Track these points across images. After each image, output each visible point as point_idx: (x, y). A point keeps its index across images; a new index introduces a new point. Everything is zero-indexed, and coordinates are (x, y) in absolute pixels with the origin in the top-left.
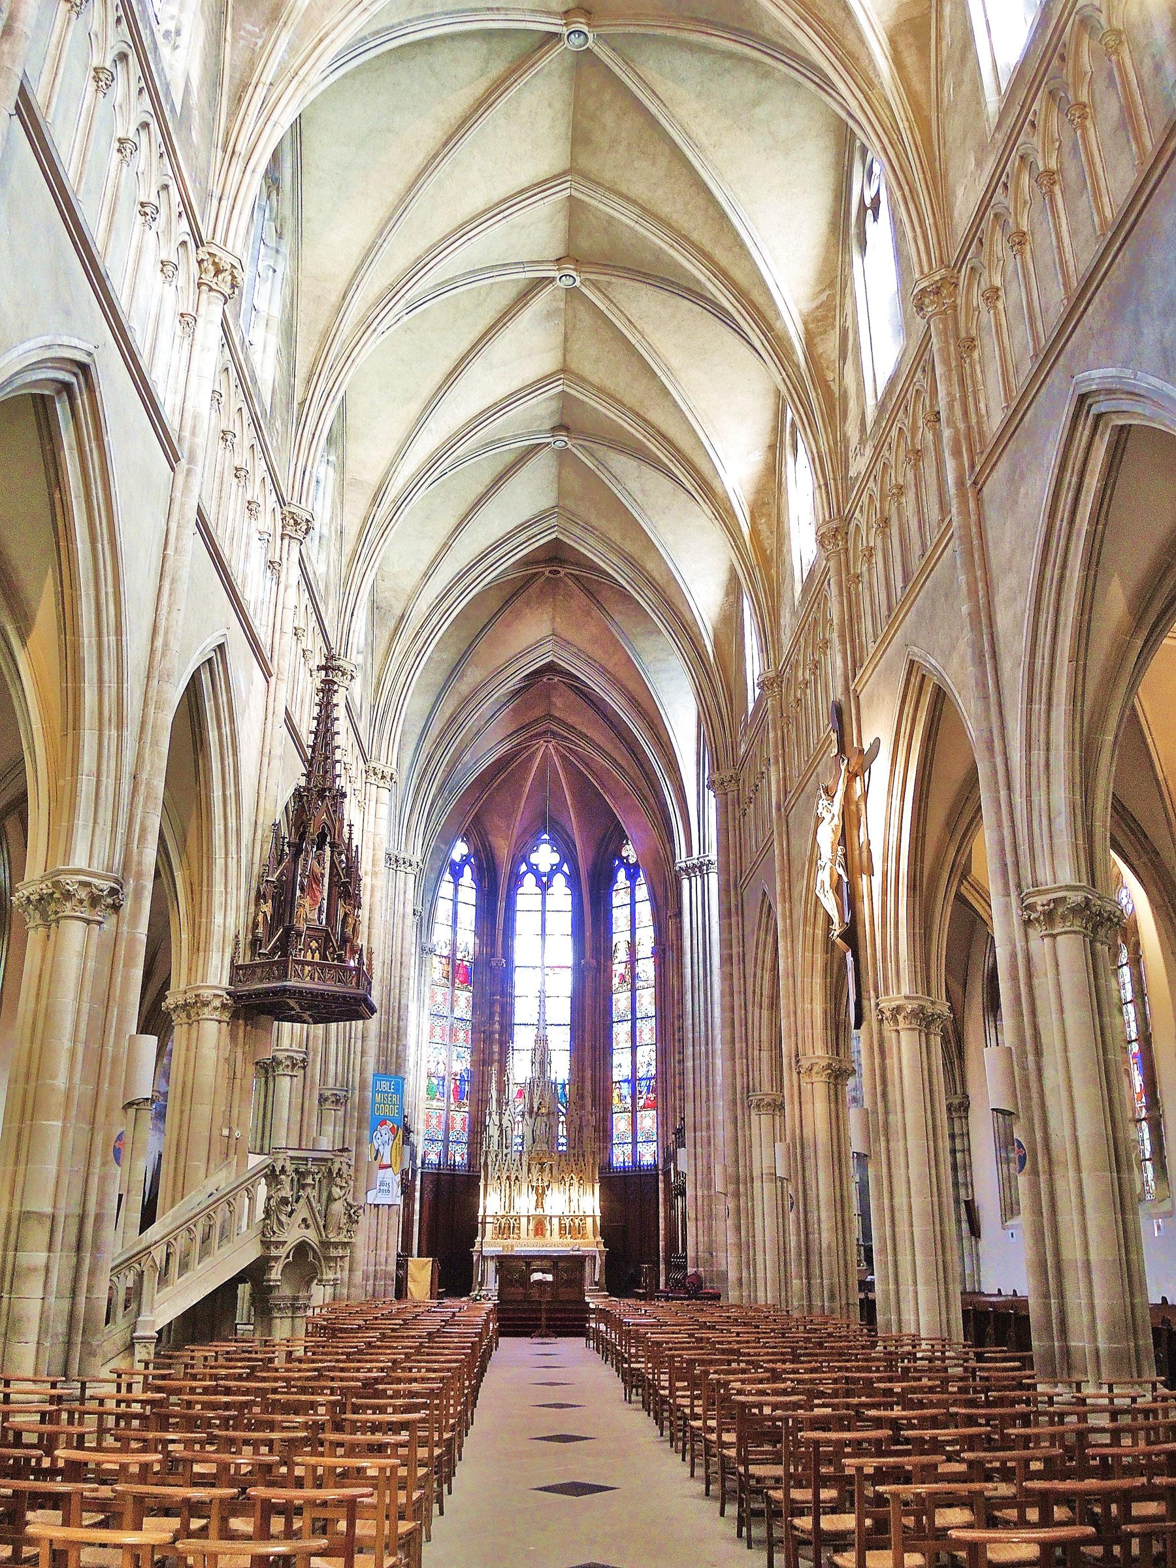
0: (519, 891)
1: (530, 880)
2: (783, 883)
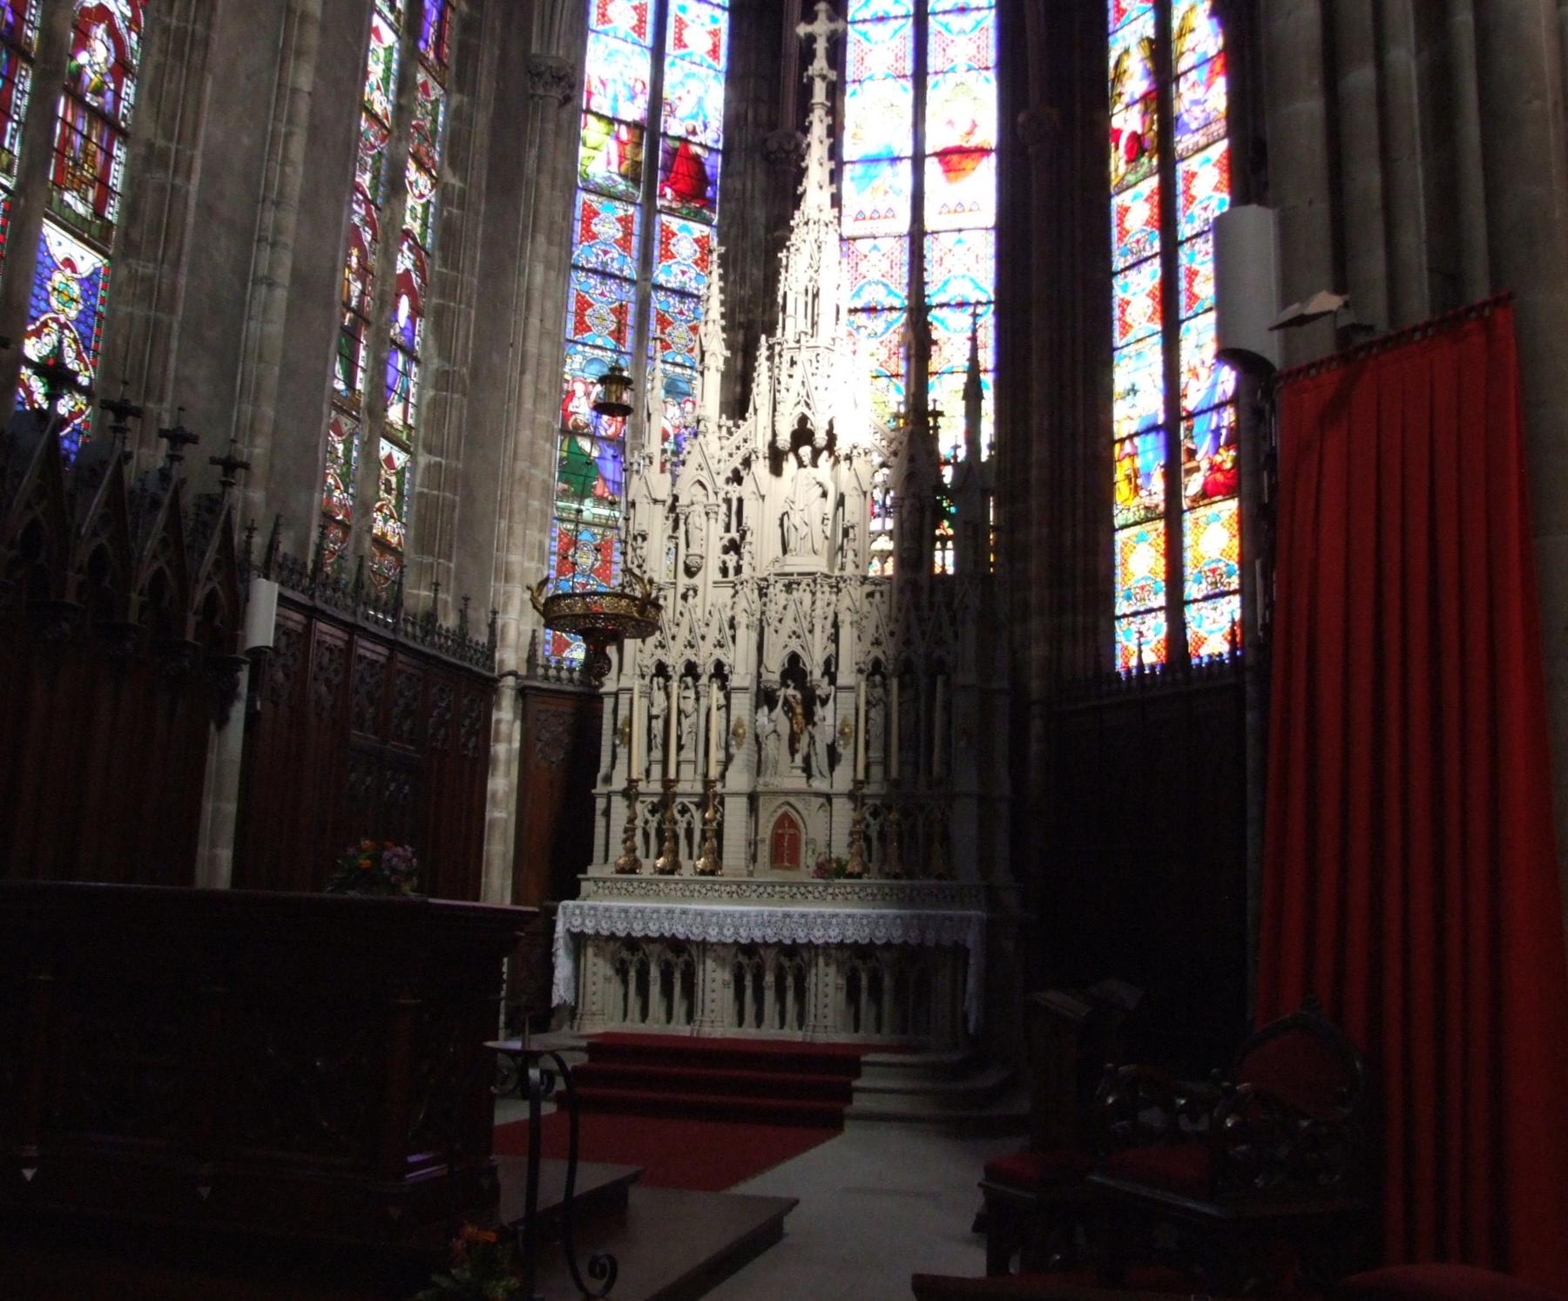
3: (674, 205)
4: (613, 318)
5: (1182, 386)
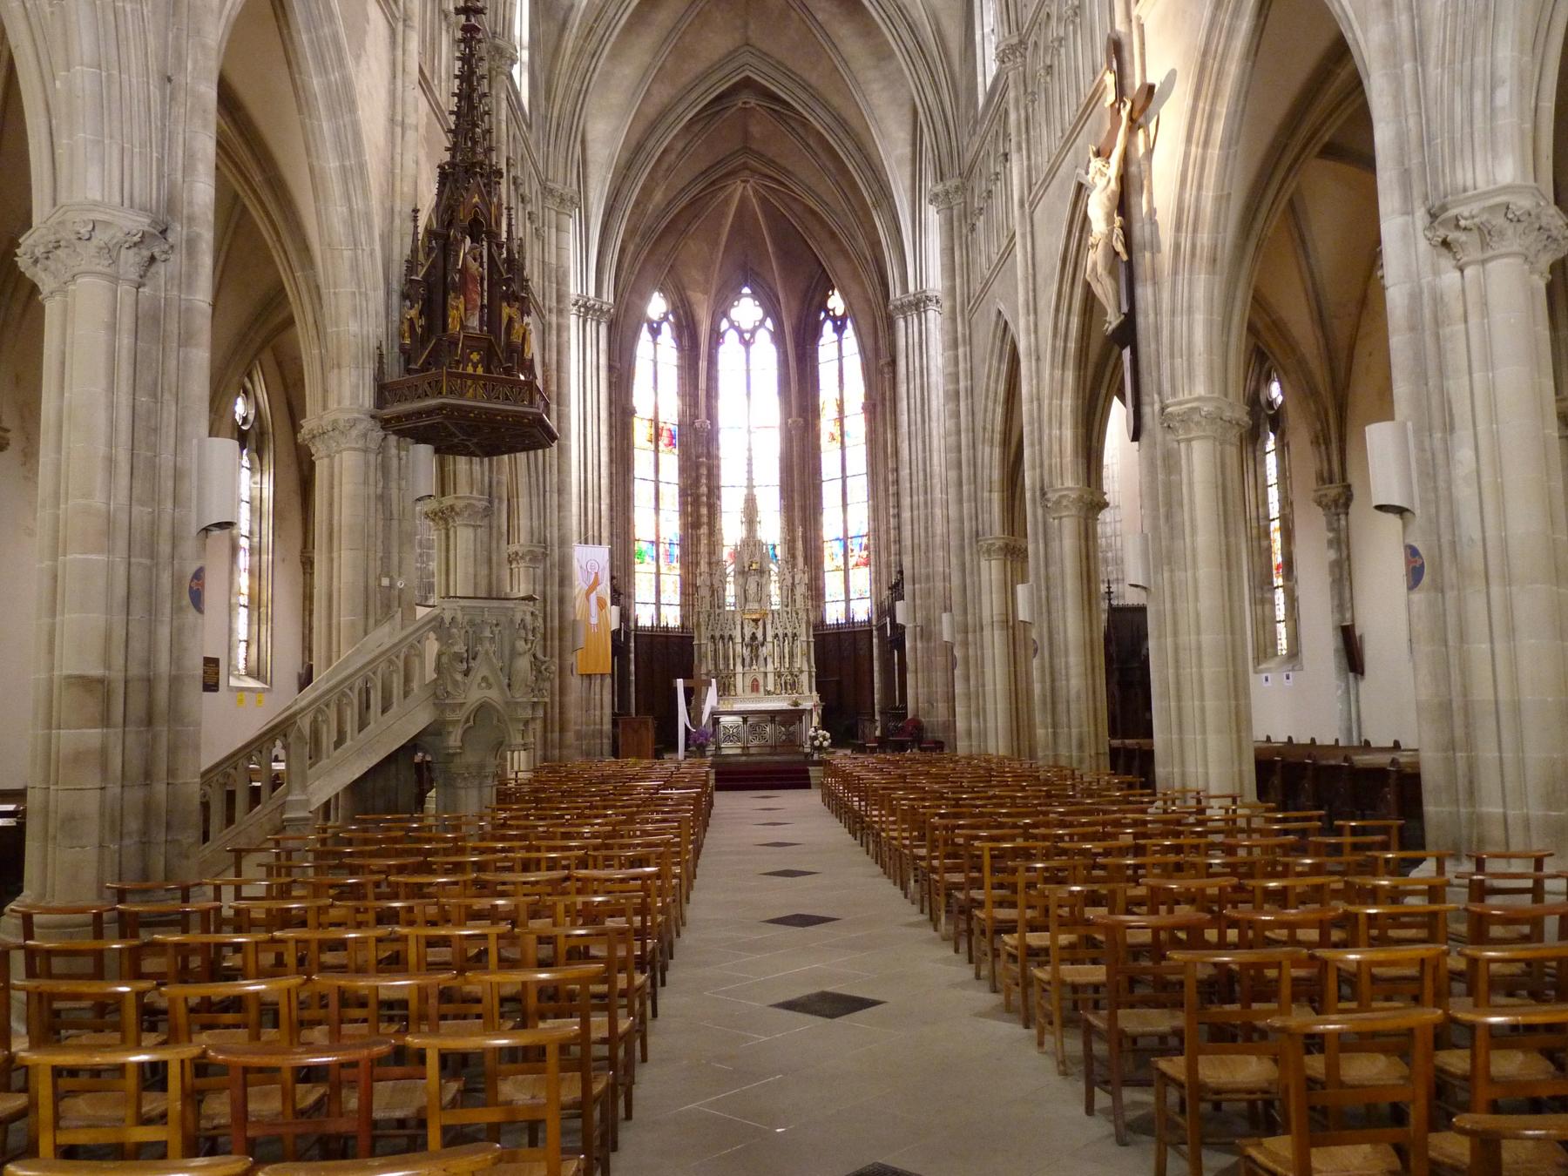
1: (731, 338)
2: (1027, 293)
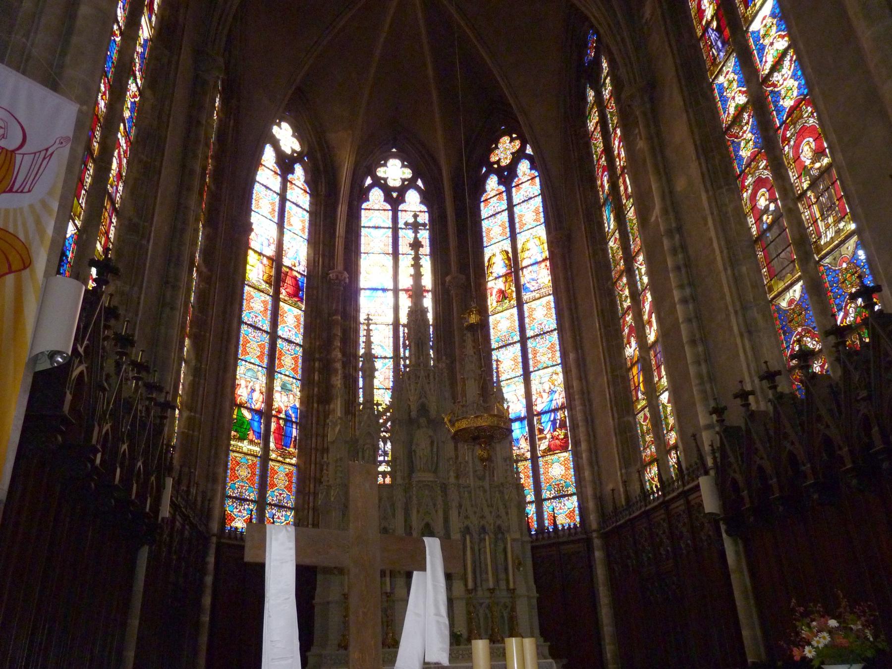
0: (364, 206)
1: (376, 195)
3: (286, 299)
4: (258, 349)
5: (534, 400)
